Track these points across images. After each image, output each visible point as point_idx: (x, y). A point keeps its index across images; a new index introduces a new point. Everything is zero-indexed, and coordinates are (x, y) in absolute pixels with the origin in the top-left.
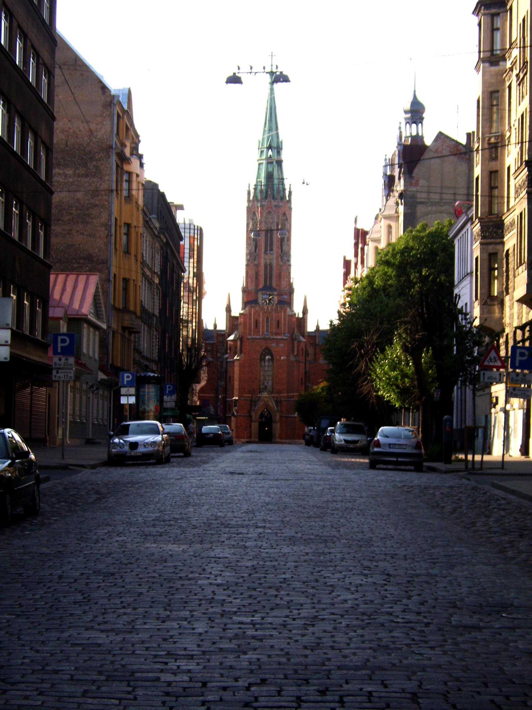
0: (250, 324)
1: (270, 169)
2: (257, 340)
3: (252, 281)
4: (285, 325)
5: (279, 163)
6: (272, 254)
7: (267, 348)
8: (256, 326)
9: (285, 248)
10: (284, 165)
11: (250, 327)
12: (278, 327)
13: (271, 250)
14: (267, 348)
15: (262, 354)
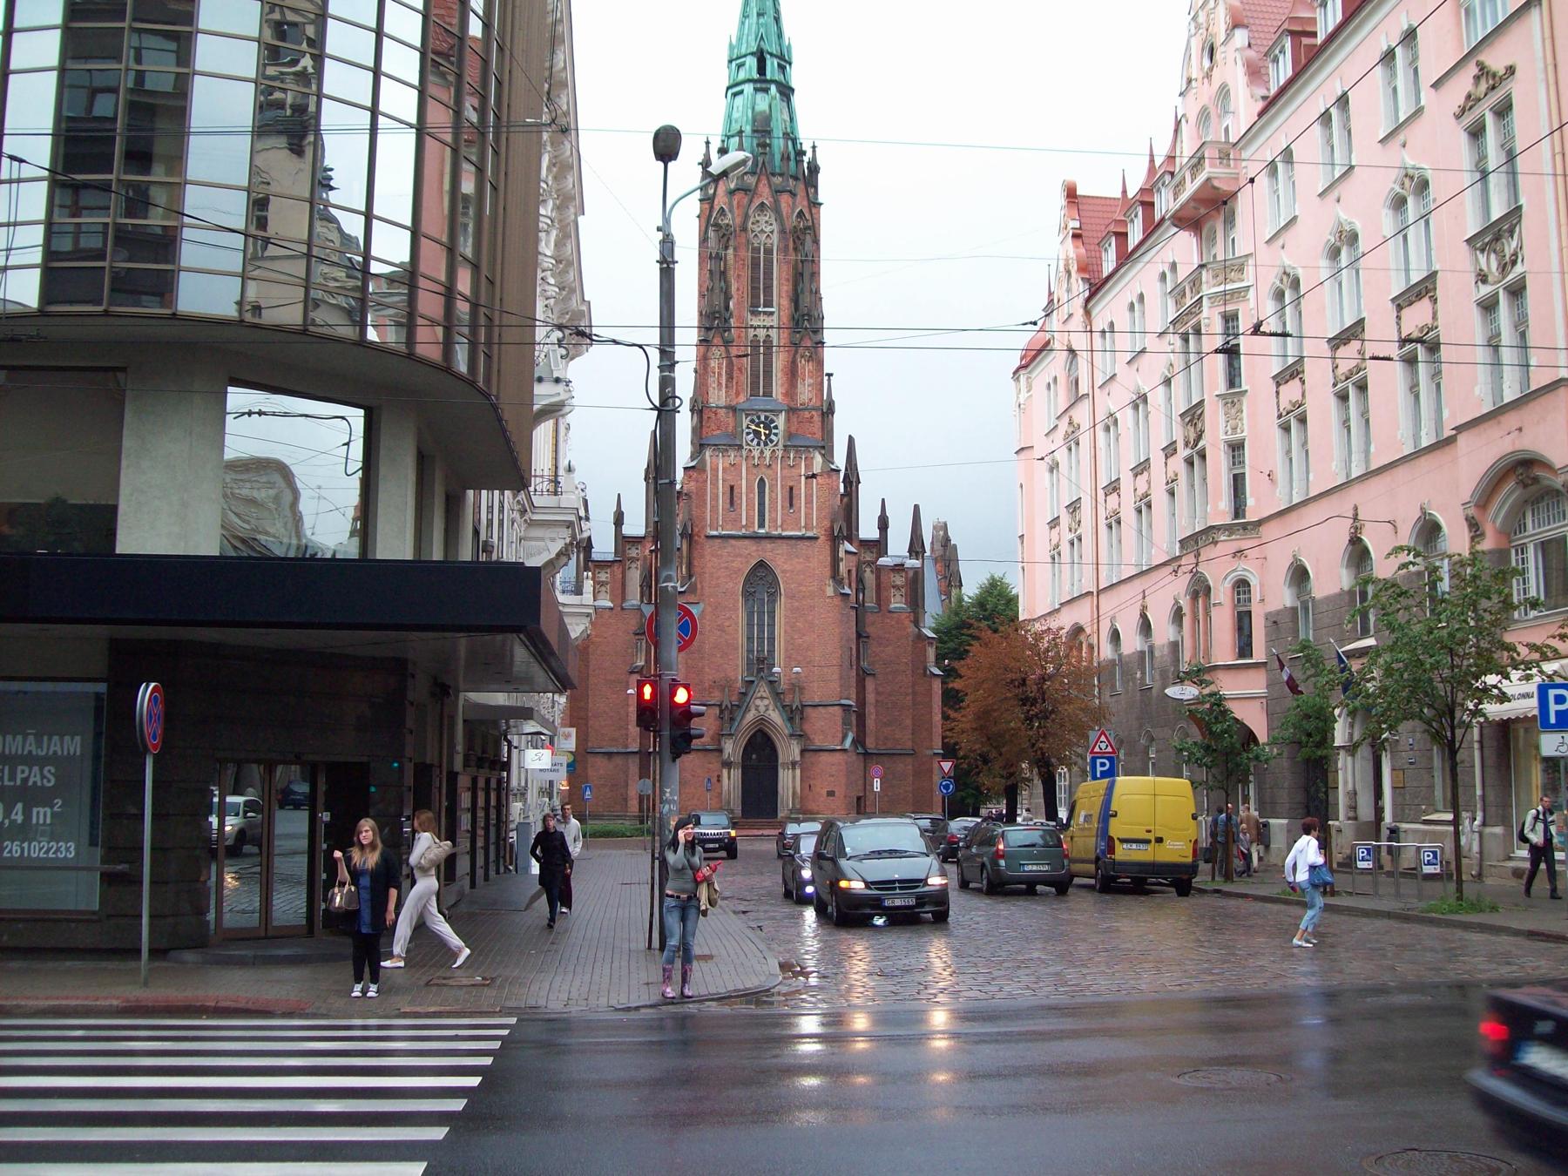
0: (715, 497)
1: (762, 103)
2: (733, 542)
3: (720, 384)
4: (809, 501)
5: (786, 92)
6: (772, 313)
7: (761, 564)
8: (732, 503)
9: (806, 300)
10: (796, 99)
11: (714, 508)
12: (791, 505)
13: (768, 304)
14: (761, 564)
15: (747, 581)
